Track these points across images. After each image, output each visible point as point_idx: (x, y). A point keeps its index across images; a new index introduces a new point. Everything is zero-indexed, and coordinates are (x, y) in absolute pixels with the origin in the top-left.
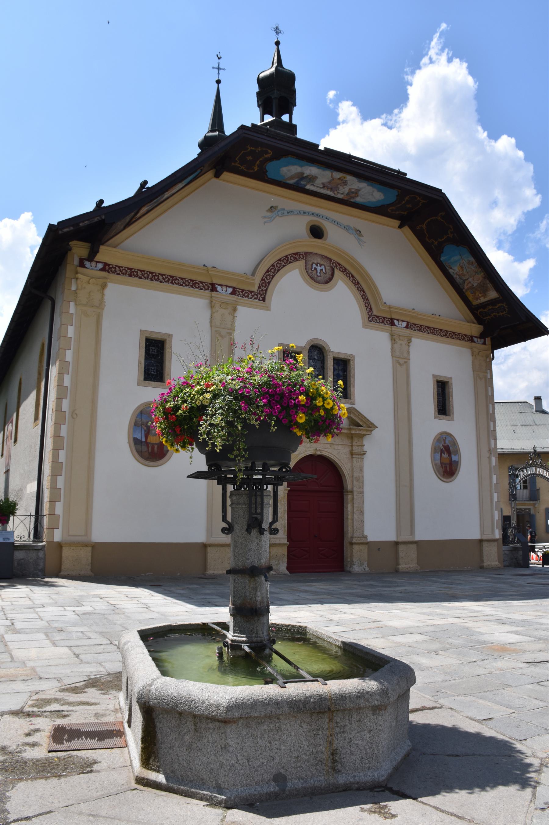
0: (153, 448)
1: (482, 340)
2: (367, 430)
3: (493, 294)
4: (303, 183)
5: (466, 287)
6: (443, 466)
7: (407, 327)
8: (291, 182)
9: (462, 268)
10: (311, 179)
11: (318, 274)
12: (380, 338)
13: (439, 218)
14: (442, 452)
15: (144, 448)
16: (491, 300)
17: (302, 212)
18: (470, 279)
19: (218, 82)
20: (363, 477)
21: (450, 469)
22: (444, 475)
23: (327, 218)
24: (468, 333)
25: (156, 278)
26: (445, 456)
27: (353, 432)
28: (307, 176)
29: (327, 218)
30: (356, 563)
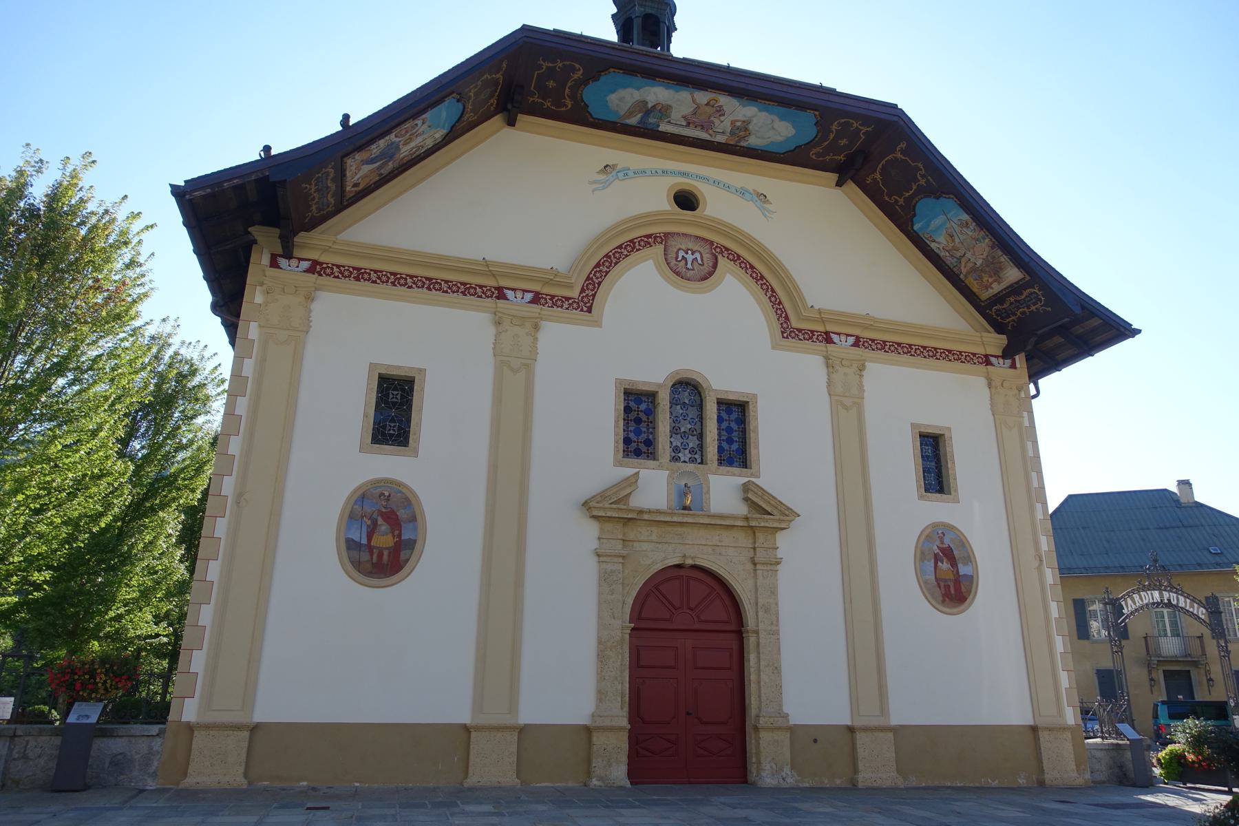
0: (380, 555)
1: (1008, 362)
2: (780, 521)
3: (1013, 275)
4: (651, 120)
5: (964, 271)
6: (942, 584)
7: (856, 344)
8: (633, 121)
9: (952, 236)
10: (663, 111)
11: (689, 266)
12: (808, 364)
13: (899, 155)
14: (937, 558)
15: (365, 556)
16: (1011, 286)
17: (660, 172)
18: (969, 255)
20: (777, 604)
21: (956, 590)
22: (943, 601)
23: (705, 179)
24: (980, 350)
25: (402, 281)
26: (945, 565)
27: (753, 523)
28: (654, 107)
29: (705, 179)
30: (768, 767)
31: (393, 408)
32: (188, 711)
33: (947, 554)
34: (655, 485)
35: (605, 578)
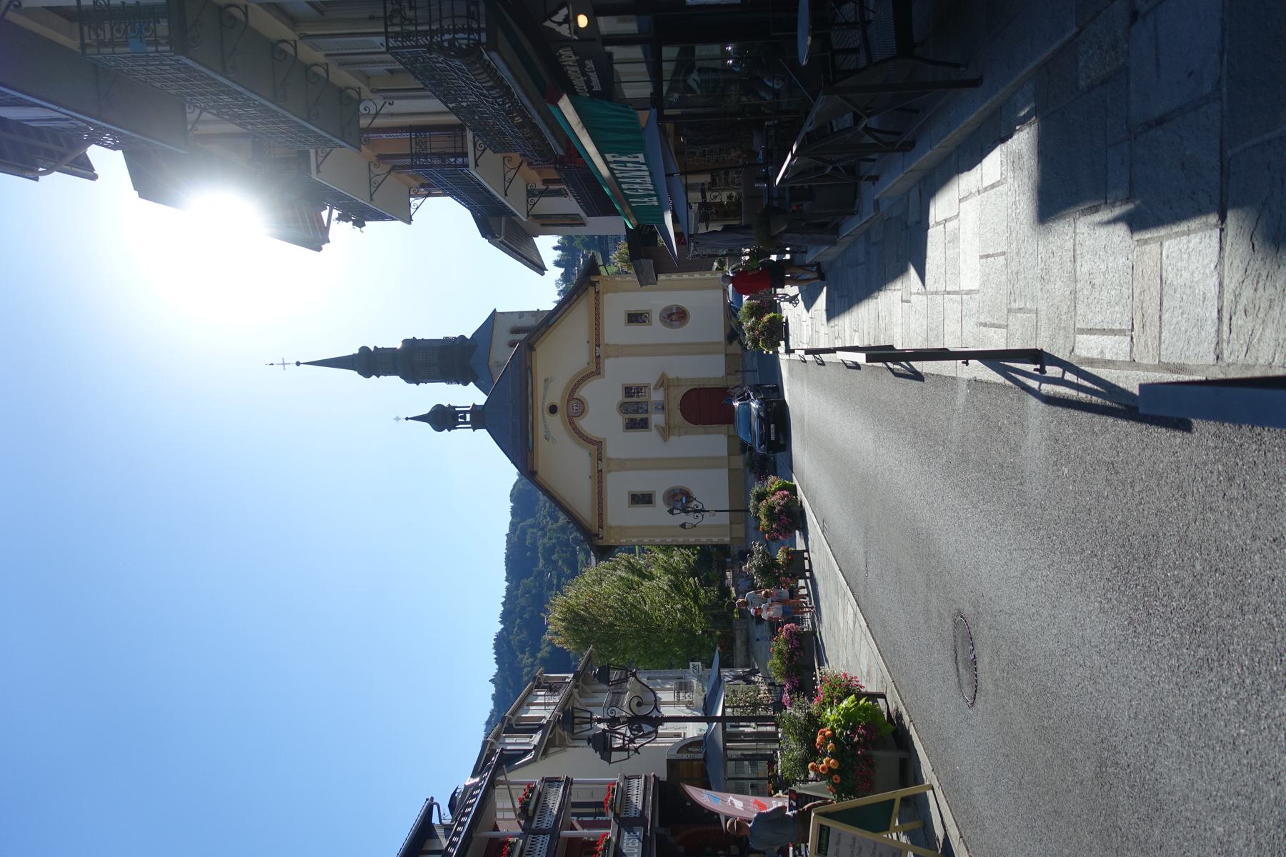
12: (609, 364)
19: (298, 364)
31: (641, 499)
32: (727, 540)
33: (670, 315)
34: (657, 419)
35: (686, 433)
